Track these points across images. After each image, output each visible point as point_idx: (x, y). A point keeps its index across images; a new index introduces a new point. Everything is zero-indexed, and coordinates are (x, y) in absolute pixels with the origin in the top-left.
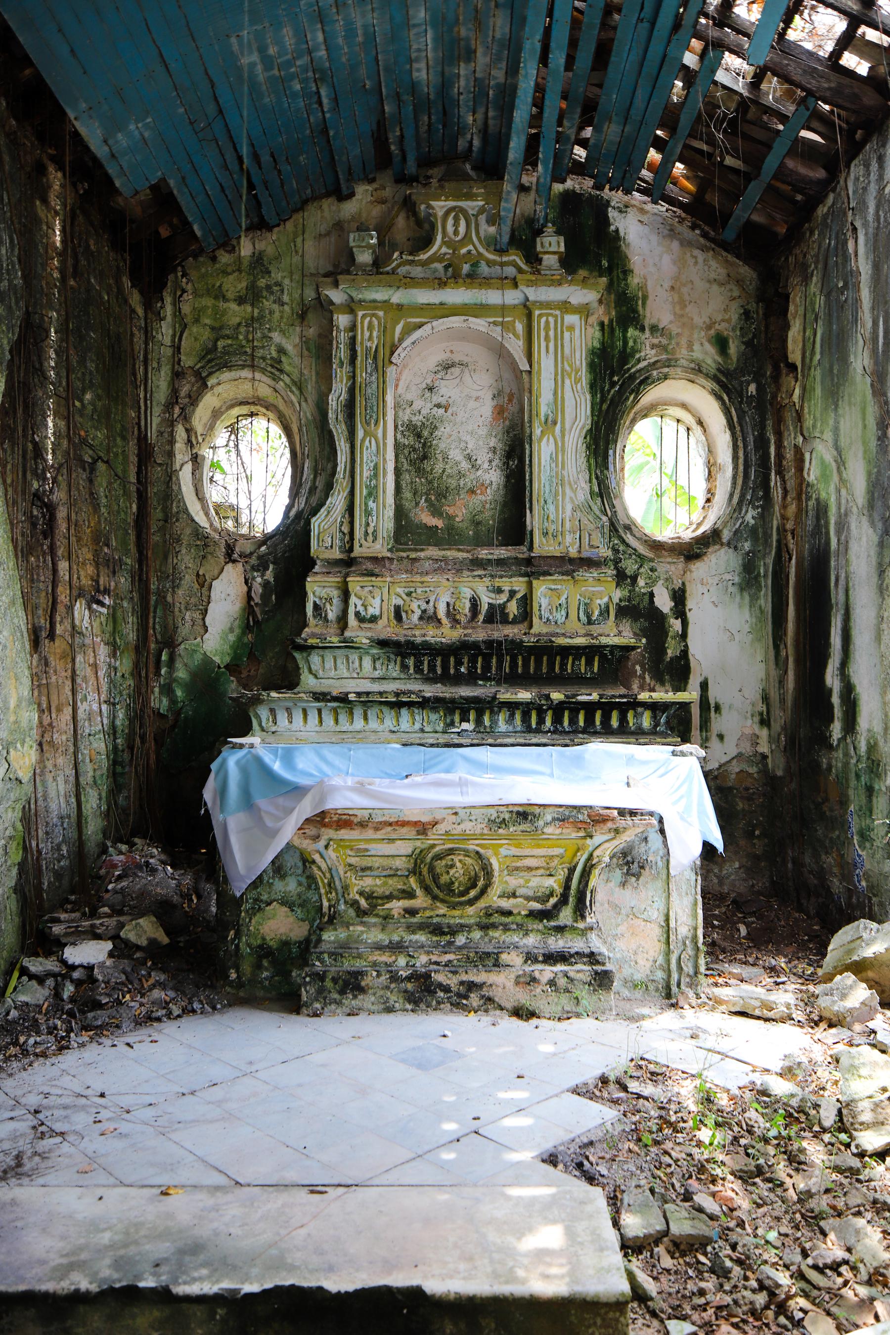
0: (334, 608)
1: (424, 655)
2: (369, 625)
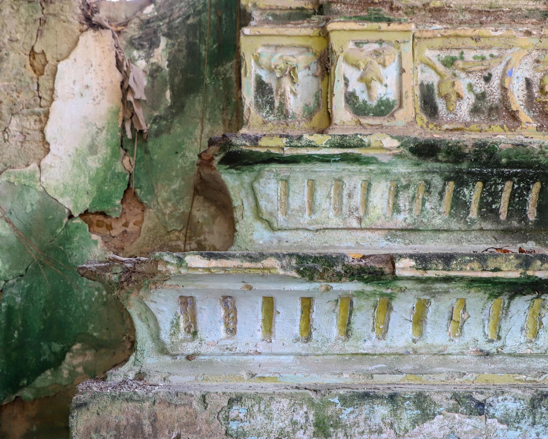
0: (299, 89)
1: (509, 178)
2: (377, 121)
